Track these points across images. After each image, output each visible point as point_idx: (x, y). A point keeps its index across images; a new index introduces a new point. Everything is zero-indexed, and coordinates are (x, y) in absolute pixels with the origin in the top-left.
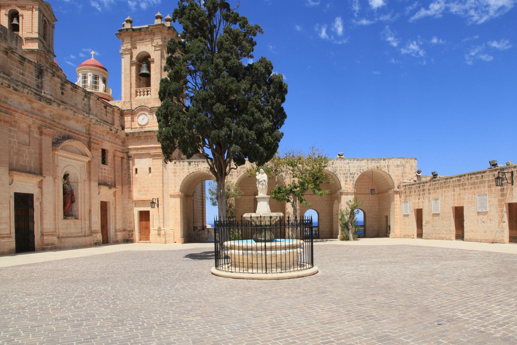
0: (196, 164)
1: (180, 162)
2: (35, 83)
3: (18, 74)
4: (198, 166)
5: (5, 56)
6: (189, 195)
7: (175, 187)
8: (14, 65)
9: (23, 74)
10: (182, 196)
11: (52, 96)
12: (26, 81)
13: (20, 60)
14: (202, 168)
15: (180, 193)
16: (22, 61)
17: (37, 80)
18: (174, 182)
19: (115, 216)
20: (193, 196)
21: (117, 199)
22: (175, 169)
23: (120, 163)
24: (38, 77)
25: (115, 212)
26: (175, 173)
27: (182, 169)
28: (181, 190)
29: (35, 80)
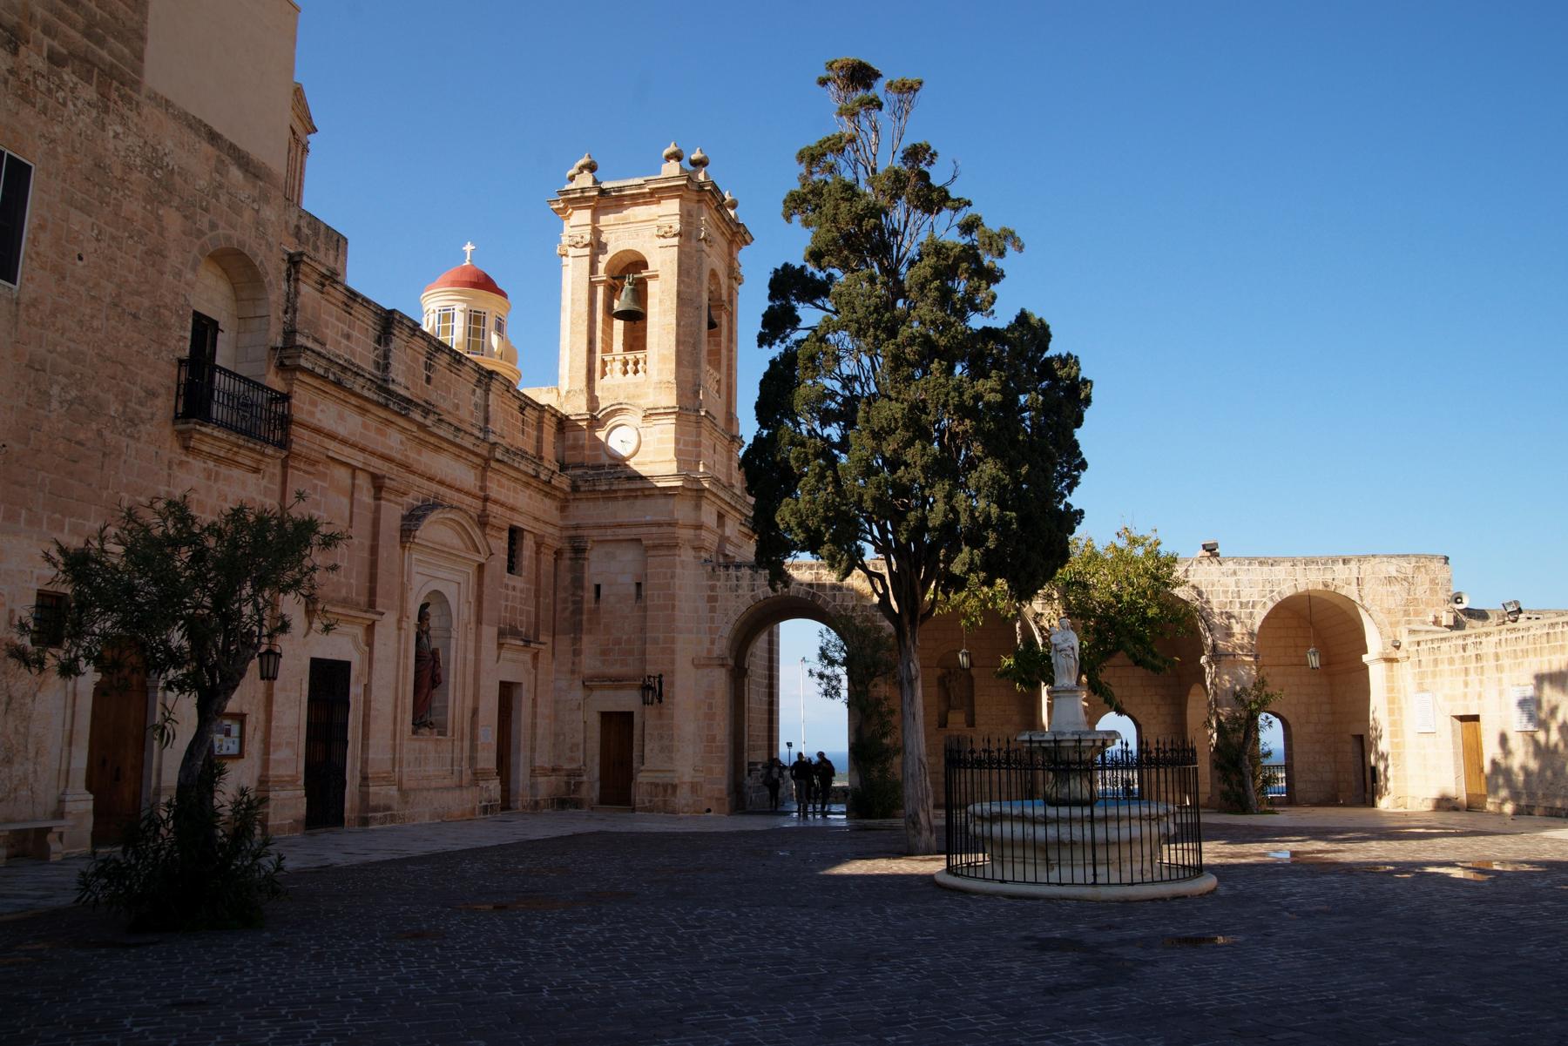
2: (372, 356)
3: (339, 338)
5: (318, 295)
8: (331, 316)
9: (348, 337)
11: (408, 389)
12: (353, 353)
13: (345, 300)
16: (350, 303)
17: (376, 349)
19: (534, 726)
21: (539, 677)
23: (552, 570)
24: (378, 342)
25: (534, 715)
29: (372, 349)
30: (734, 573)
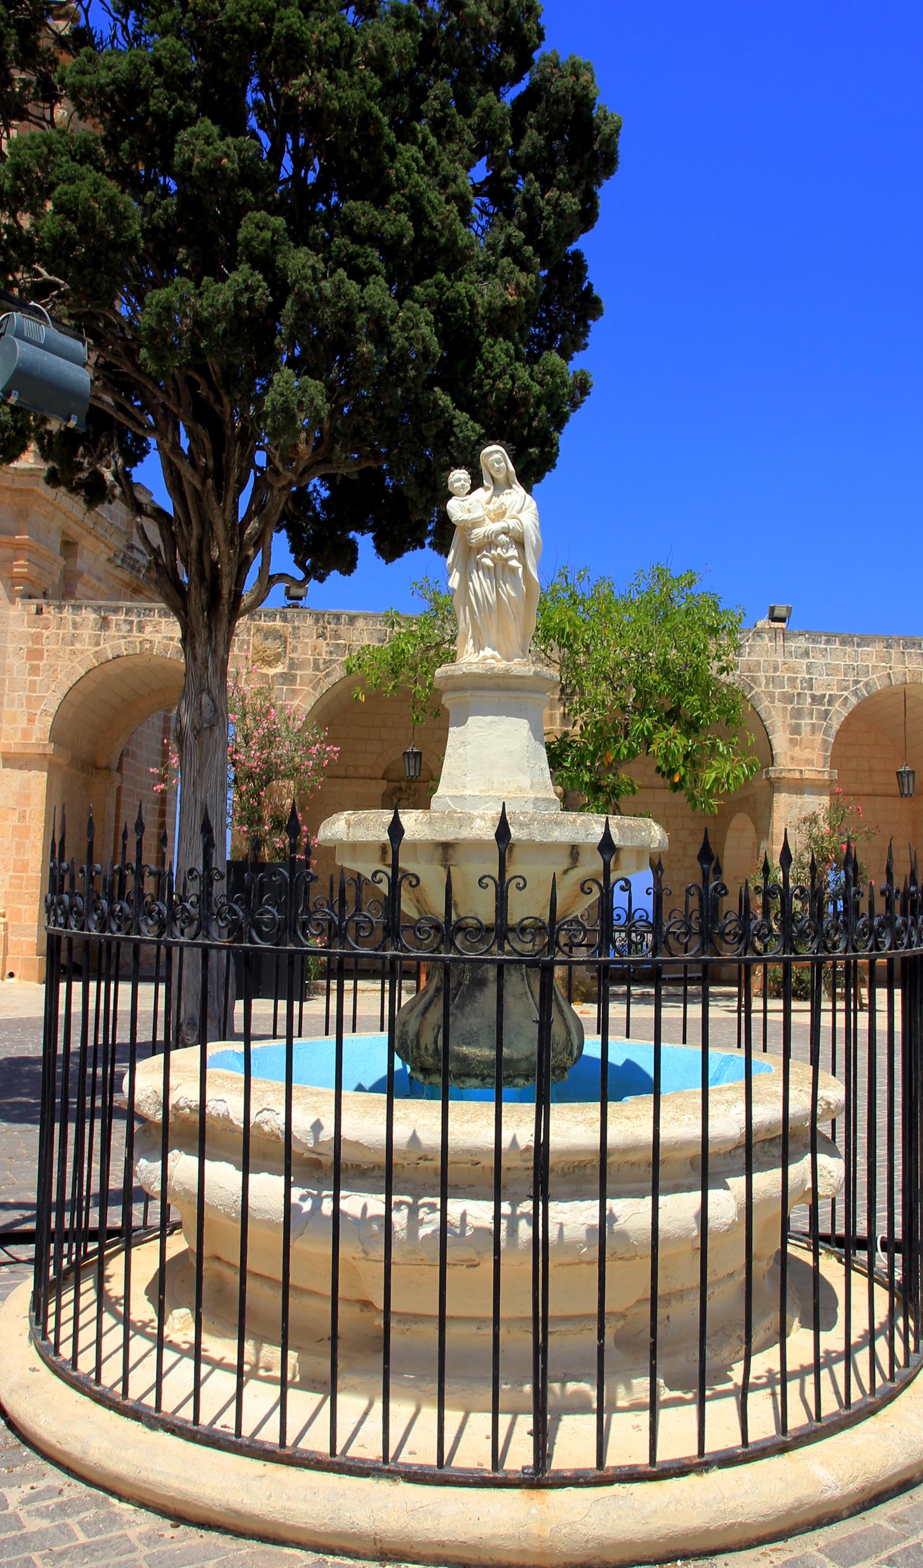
0: (135, 619)
1: (60, 608)
4: (141, 629)
6: (102, 762)
7: (31, 720)
10: (61, 761)
14: (157, 638)
15: (50, 749)
18: (29, 698)
20: (119, 769)
22: (37, 638)
26: (35, 654)
27: (68, 638)
28: (56, 735)
30: (70, 617)
